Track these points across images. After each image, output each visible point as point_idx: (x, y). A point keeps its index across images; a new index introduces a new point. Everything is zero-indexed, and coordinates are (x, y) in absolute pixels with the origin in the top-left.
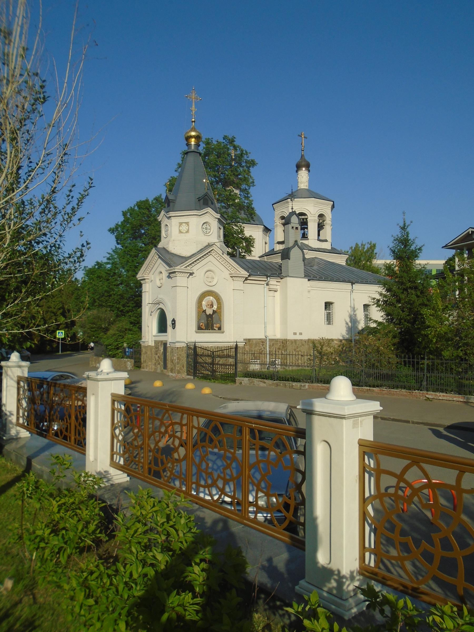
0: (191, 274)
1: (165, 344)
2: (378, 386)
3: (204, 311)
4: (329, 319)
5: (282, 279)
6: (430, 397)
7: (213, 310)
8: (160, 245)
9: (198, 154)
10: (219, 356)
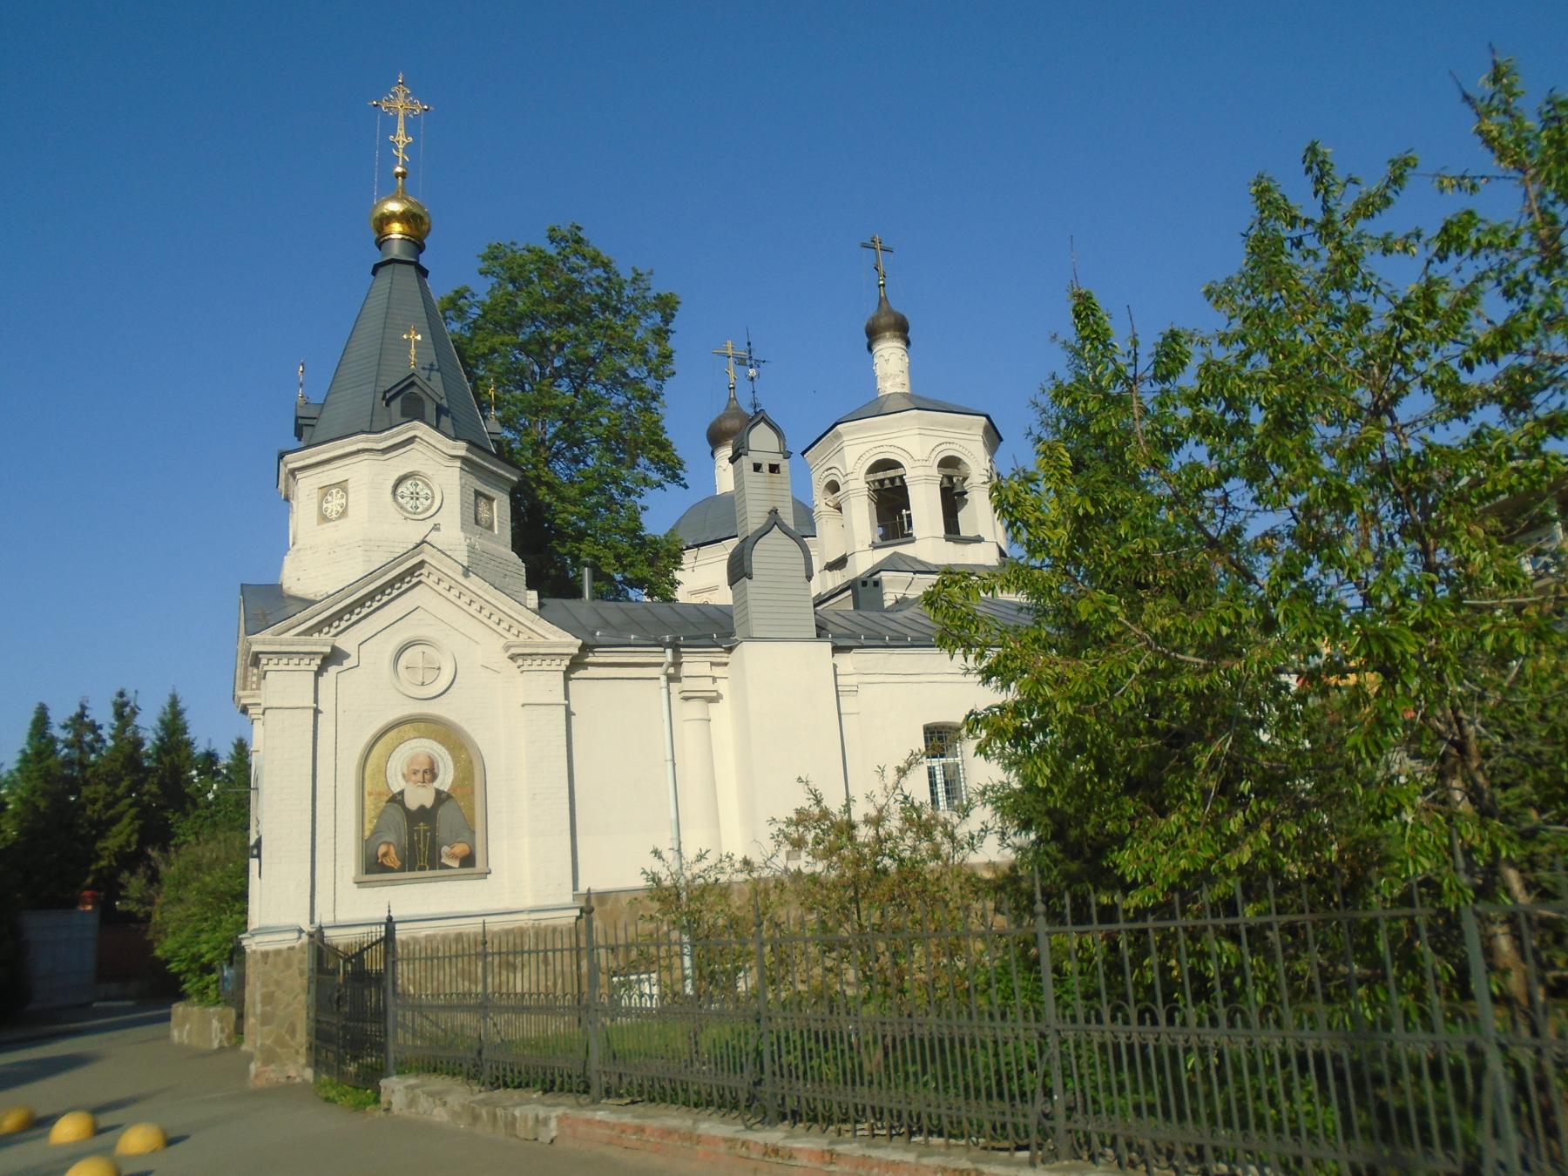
0: (334, 657)
5: (730, 650)
7: (438, 793)
9: (412, 269)
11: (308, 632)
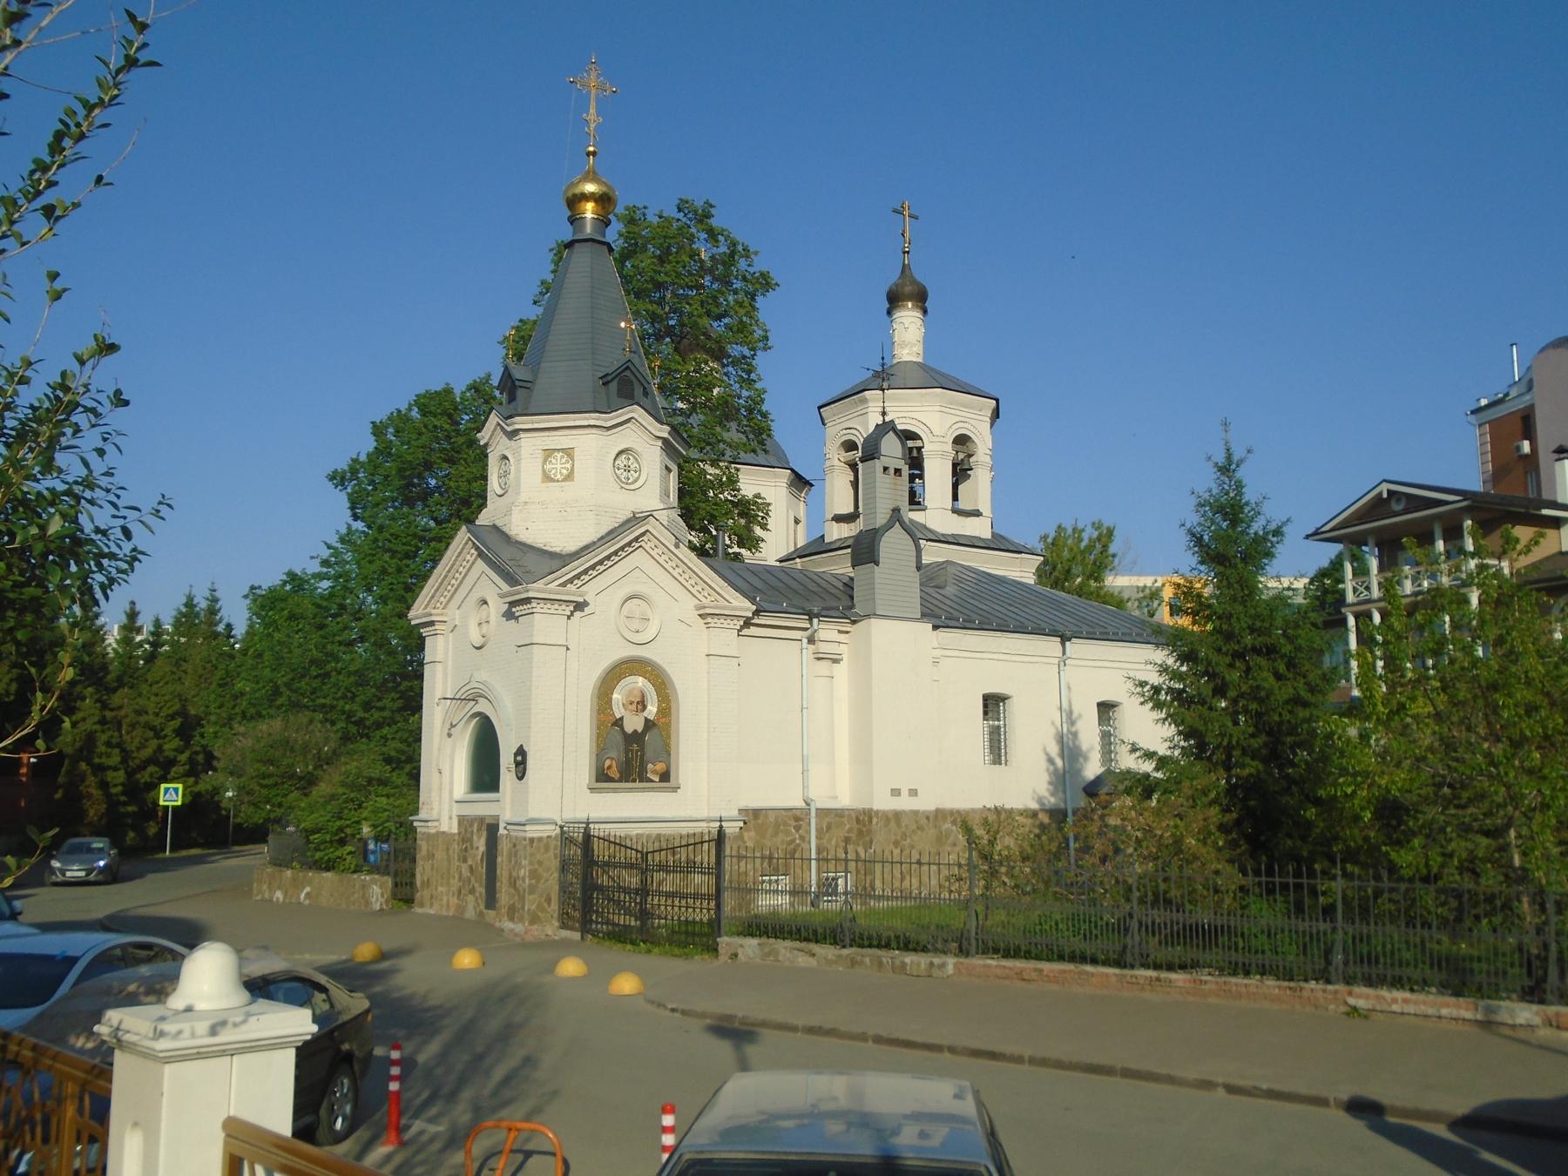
0: (580, 606)
1: (492, 829)
2: (1183, 967)
3: (619, 723)
4: (997, 748)
5: (854, 622)
6: (1361, 1003)
8: (483, 519)
9: (605, 248)
10: (663, 868)
11: (564, 585)
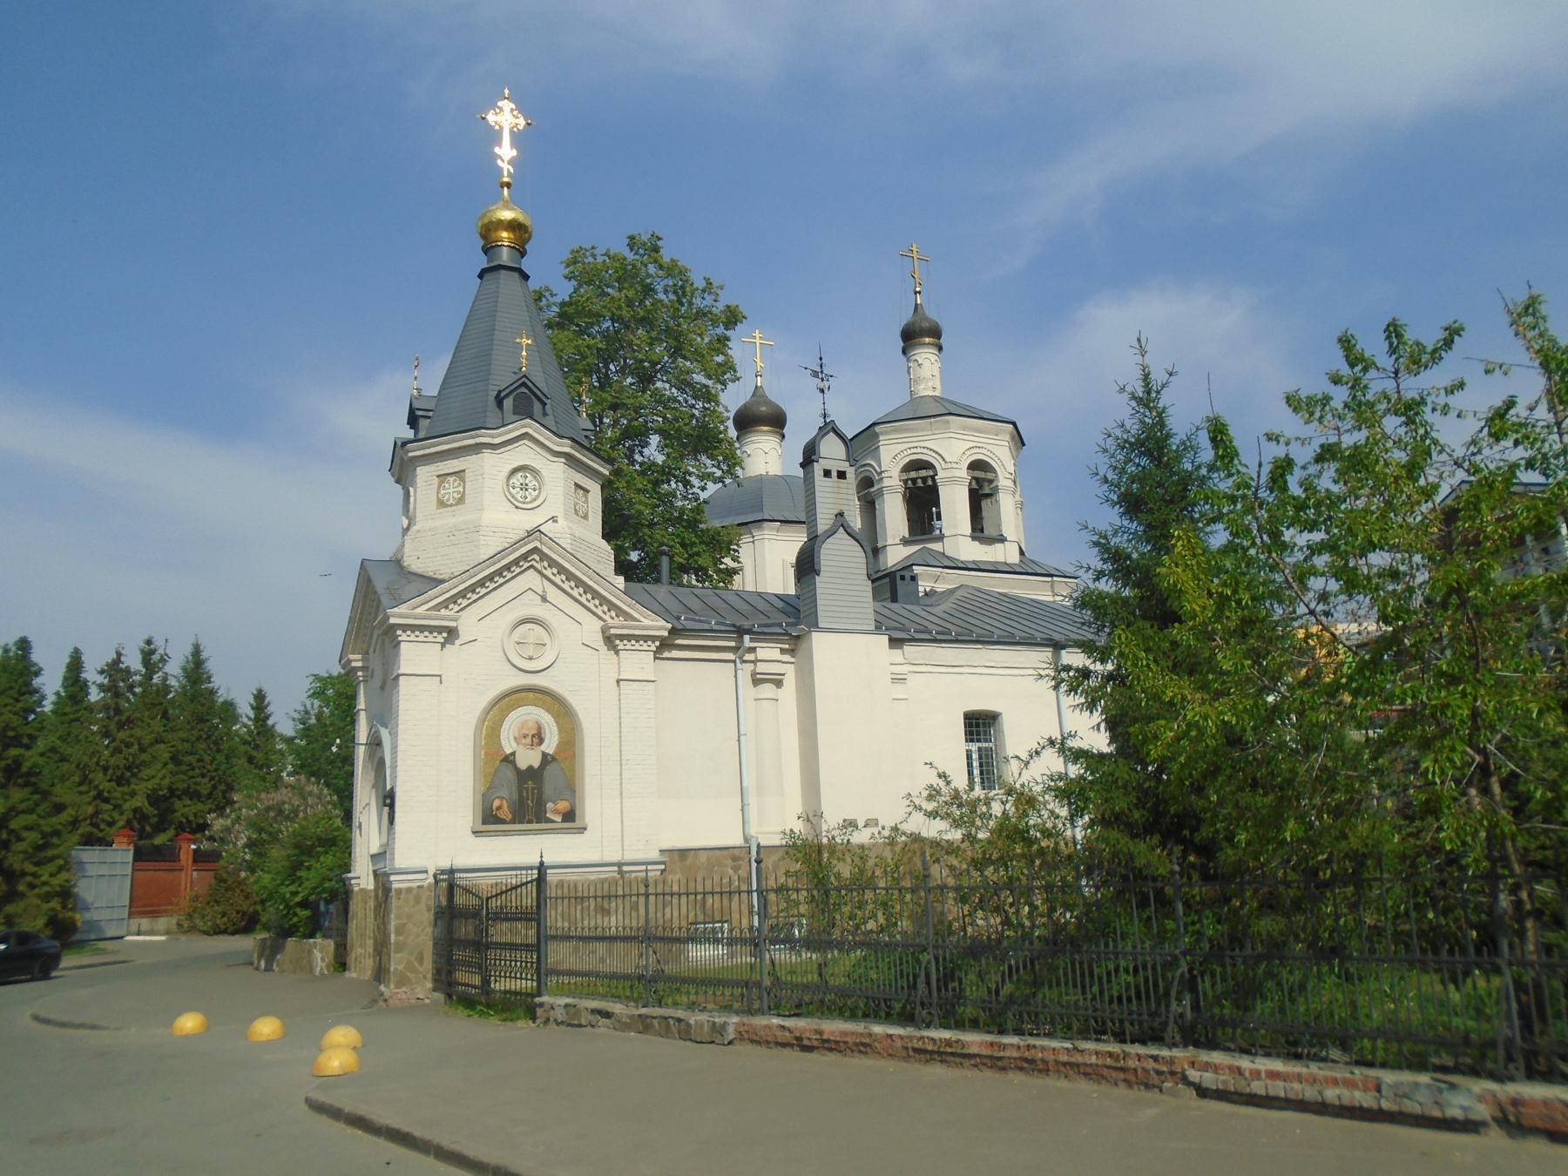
7: (544, 755)
9: (516, 275)
